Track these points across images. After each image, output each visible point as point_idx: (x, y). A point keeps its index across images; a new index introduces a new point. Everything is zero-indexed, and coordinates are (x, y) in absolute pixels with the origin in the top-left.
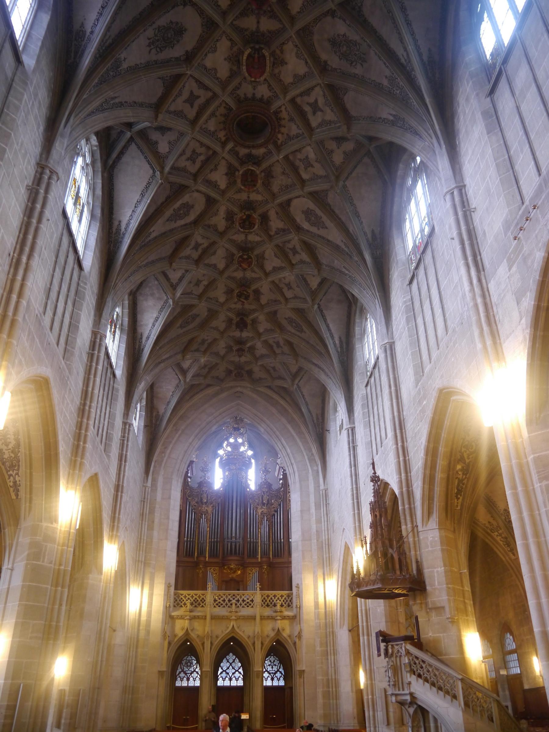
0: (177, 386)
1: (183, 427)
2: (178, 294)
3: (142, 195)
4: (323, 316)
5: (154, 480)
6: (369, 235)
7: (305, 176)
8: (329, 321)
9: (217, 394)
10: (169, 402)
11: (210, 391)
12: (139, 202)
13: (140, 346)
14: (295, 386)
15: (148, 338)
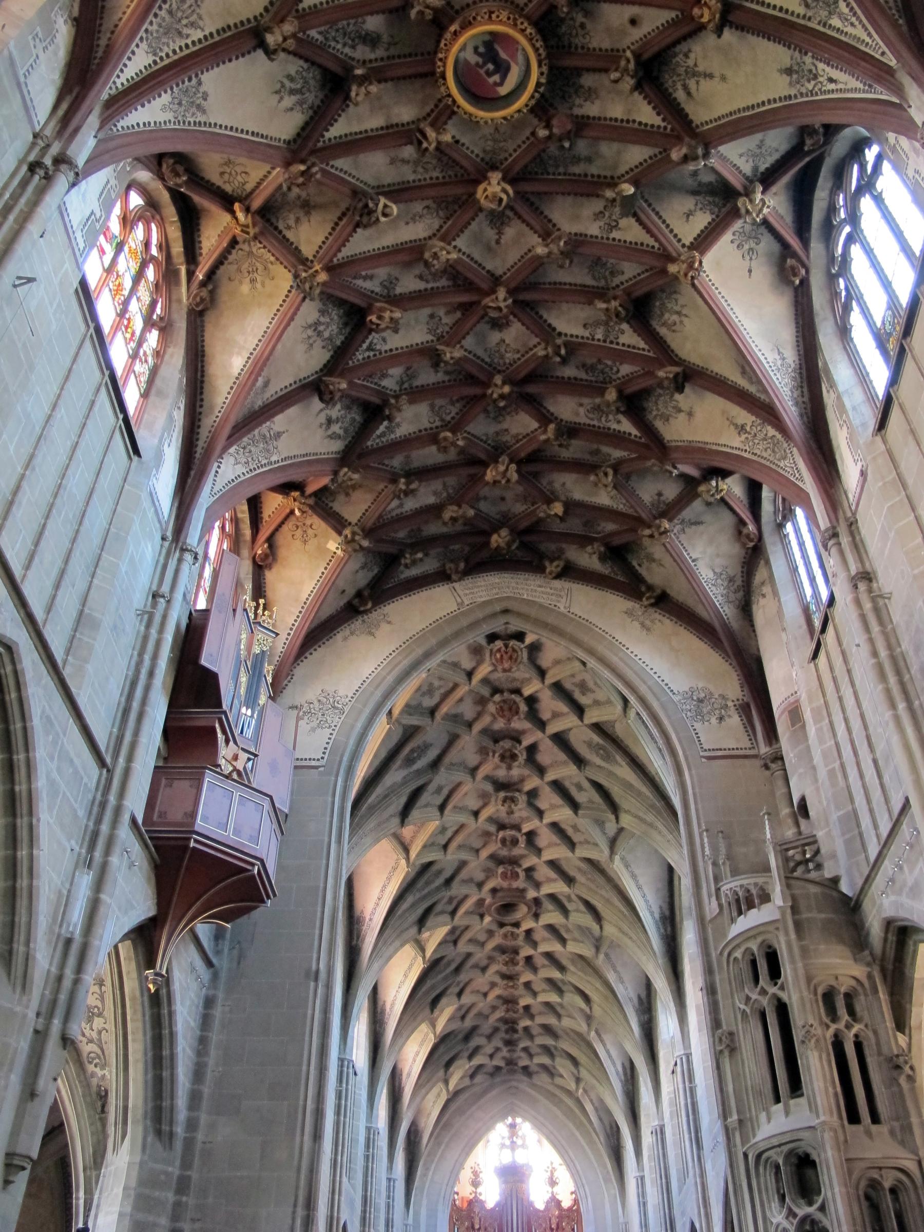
0: (439, 1095)
1: (446, 1140)
2: (441, 1024)
3: (406, 976)
4: (602, 1041)
5: (417, 1214)
6: (636, 1000)
7: (565, 936)
8: (609, 1046)
9: (485, 1092)
10: (430, 1114)
11: (476, 1089)
12: (402, 982)
13: (400, 1084)
14: (581, 1091)
15: (409, 1074)
